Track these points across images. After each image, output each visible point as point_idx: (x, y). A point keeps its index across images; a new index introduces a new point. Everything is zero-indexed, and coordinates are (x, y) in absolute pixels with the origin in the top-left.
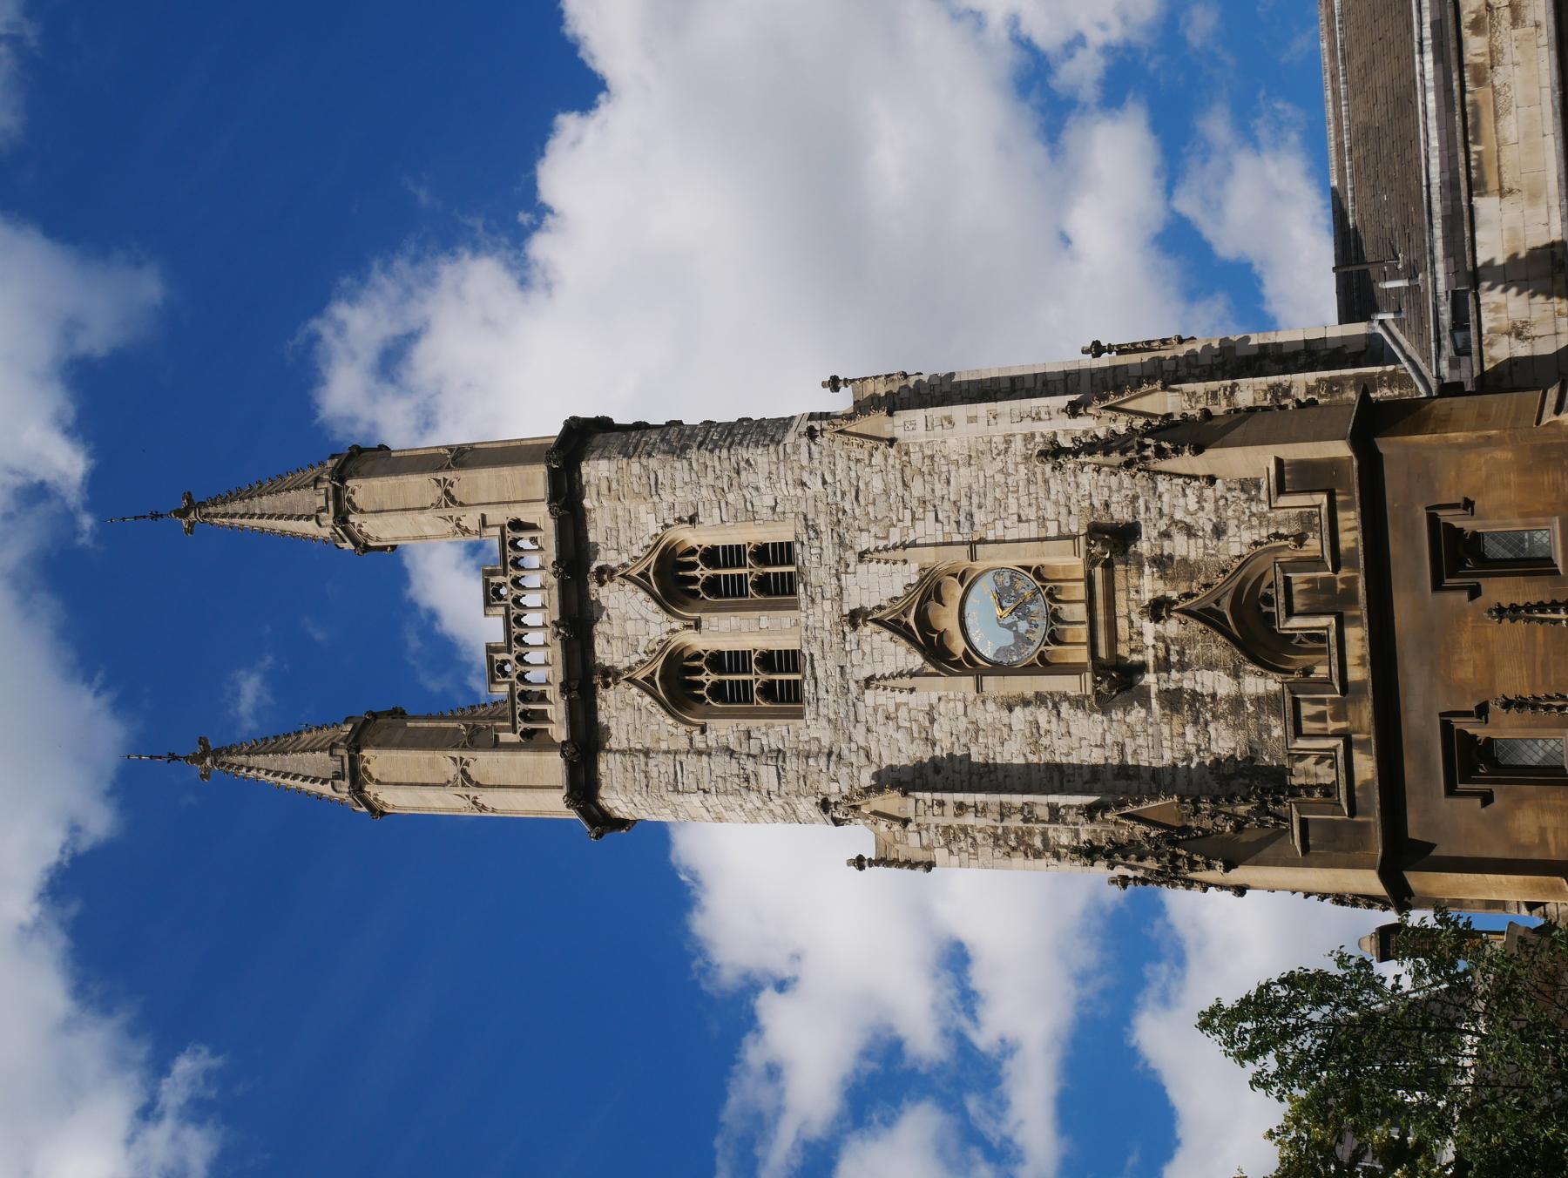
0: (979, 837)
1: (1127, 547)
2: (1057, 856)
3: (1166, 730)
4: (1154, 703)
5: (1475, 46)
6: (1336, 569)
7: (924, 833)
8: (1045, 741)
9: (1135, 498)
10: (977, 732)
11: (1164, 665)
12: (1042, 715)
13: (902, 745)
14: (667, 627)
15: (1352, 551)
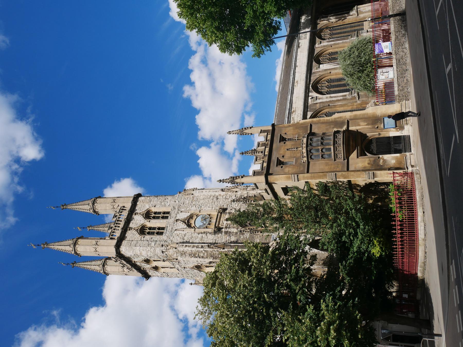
0: (187, 254)
1: (225, 211)
2: (200, 258)
3: (224, 237)
4: (223, 233)
6: (266, 141)
7: (177, 254)
8: (203, 239)
9: (228, 205)
10: (192, 237)
11: (226, 228)
12: (204, 235)
13: (178, 240)
14: (144, 221)
15: (269, 140)
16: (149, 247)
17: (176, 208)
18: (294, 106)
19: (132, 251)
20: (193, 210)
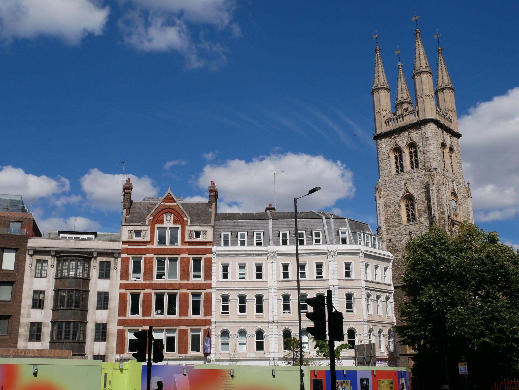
16: (437, 154)
19: (431, 135)
20: (459, 197)
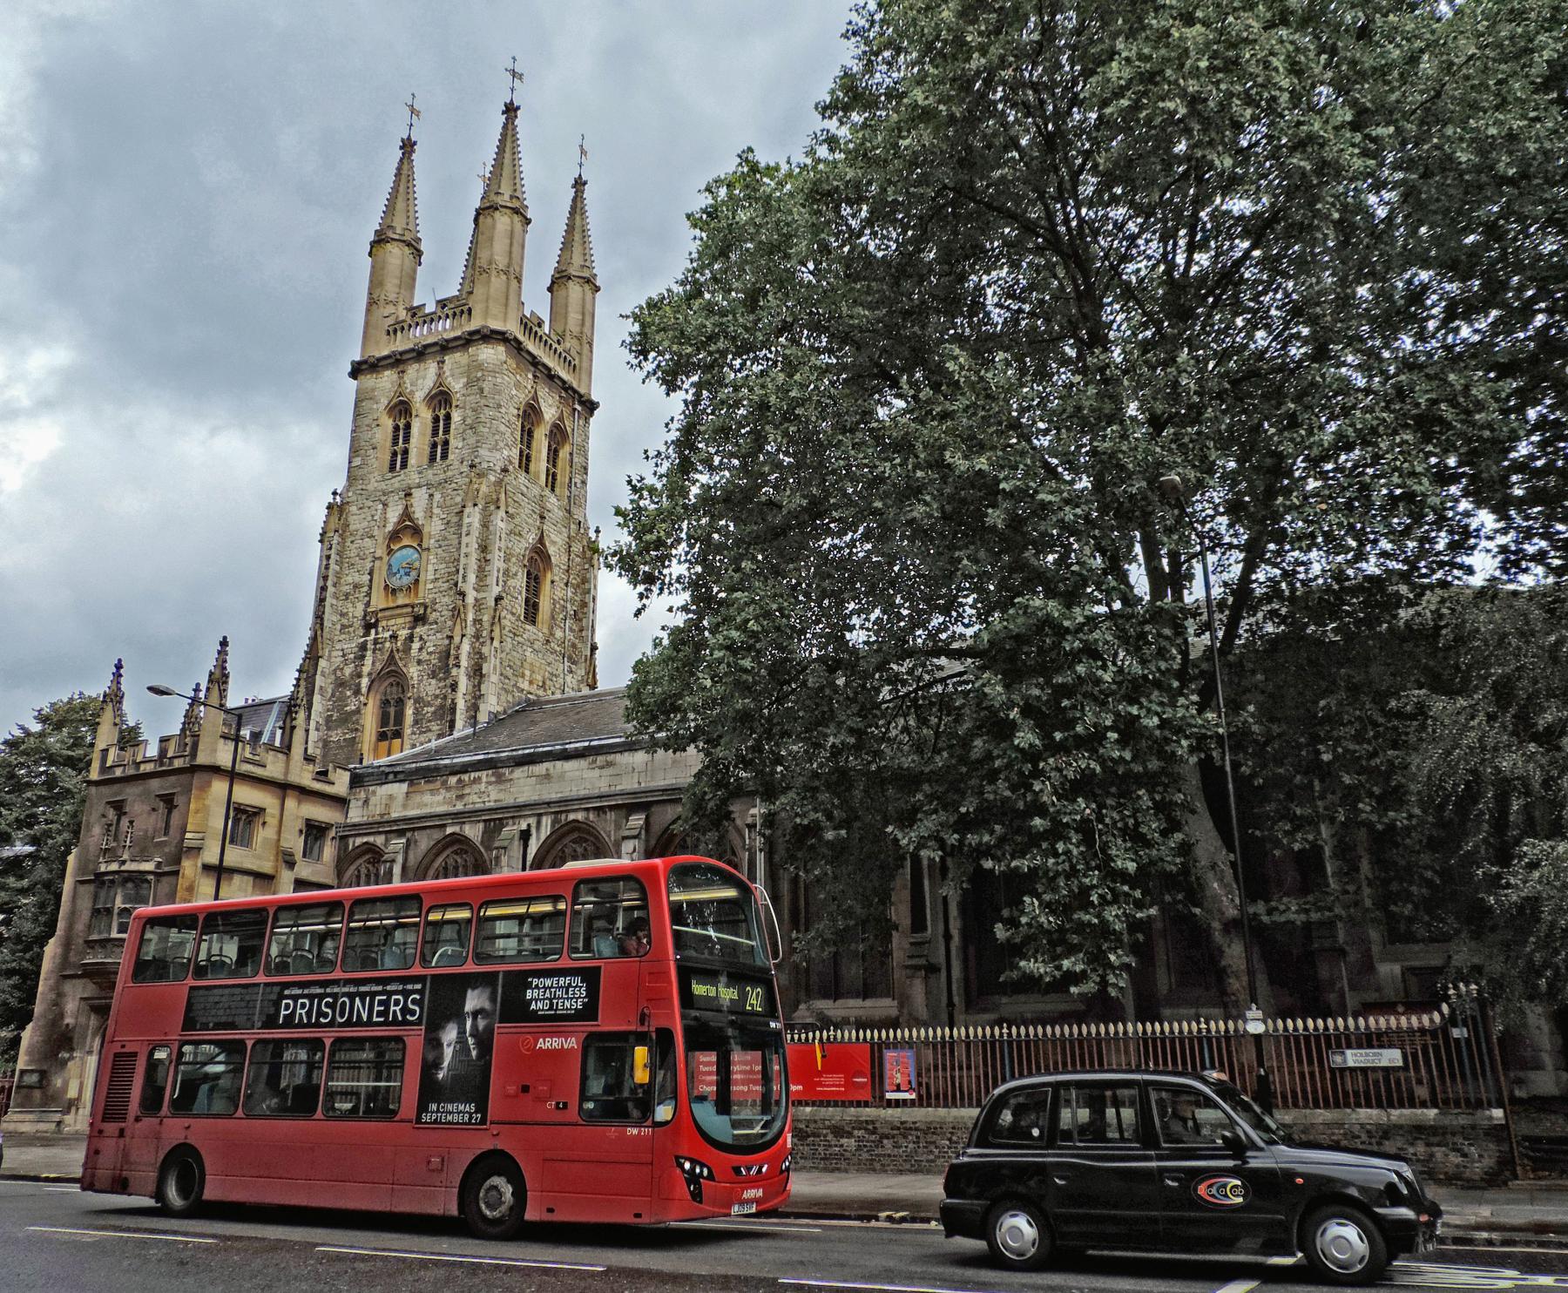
5: (453, 780)
17: (449, 473)
18: (519, 773)
20: (434, 529)
